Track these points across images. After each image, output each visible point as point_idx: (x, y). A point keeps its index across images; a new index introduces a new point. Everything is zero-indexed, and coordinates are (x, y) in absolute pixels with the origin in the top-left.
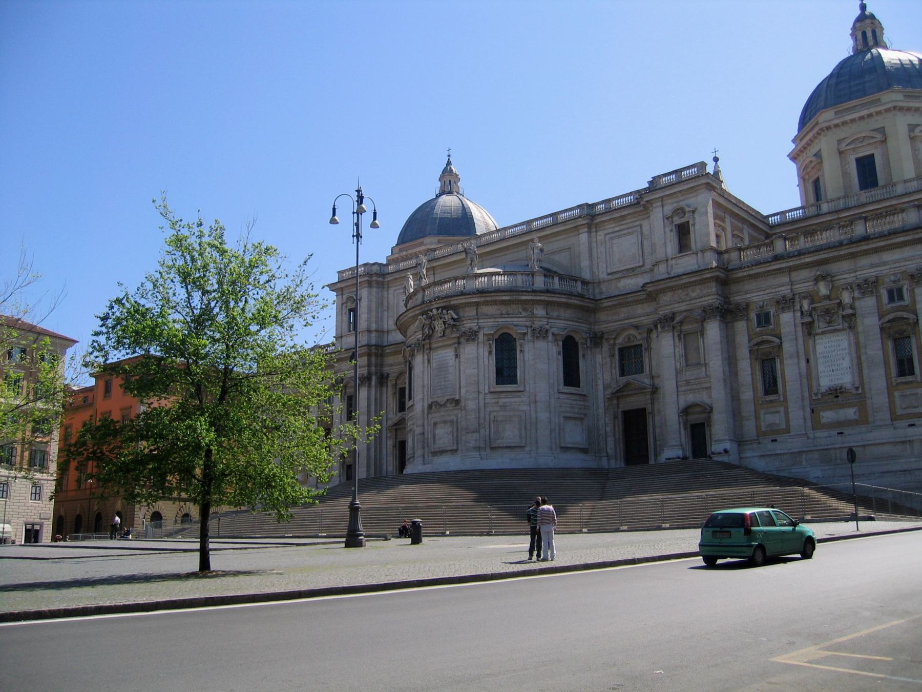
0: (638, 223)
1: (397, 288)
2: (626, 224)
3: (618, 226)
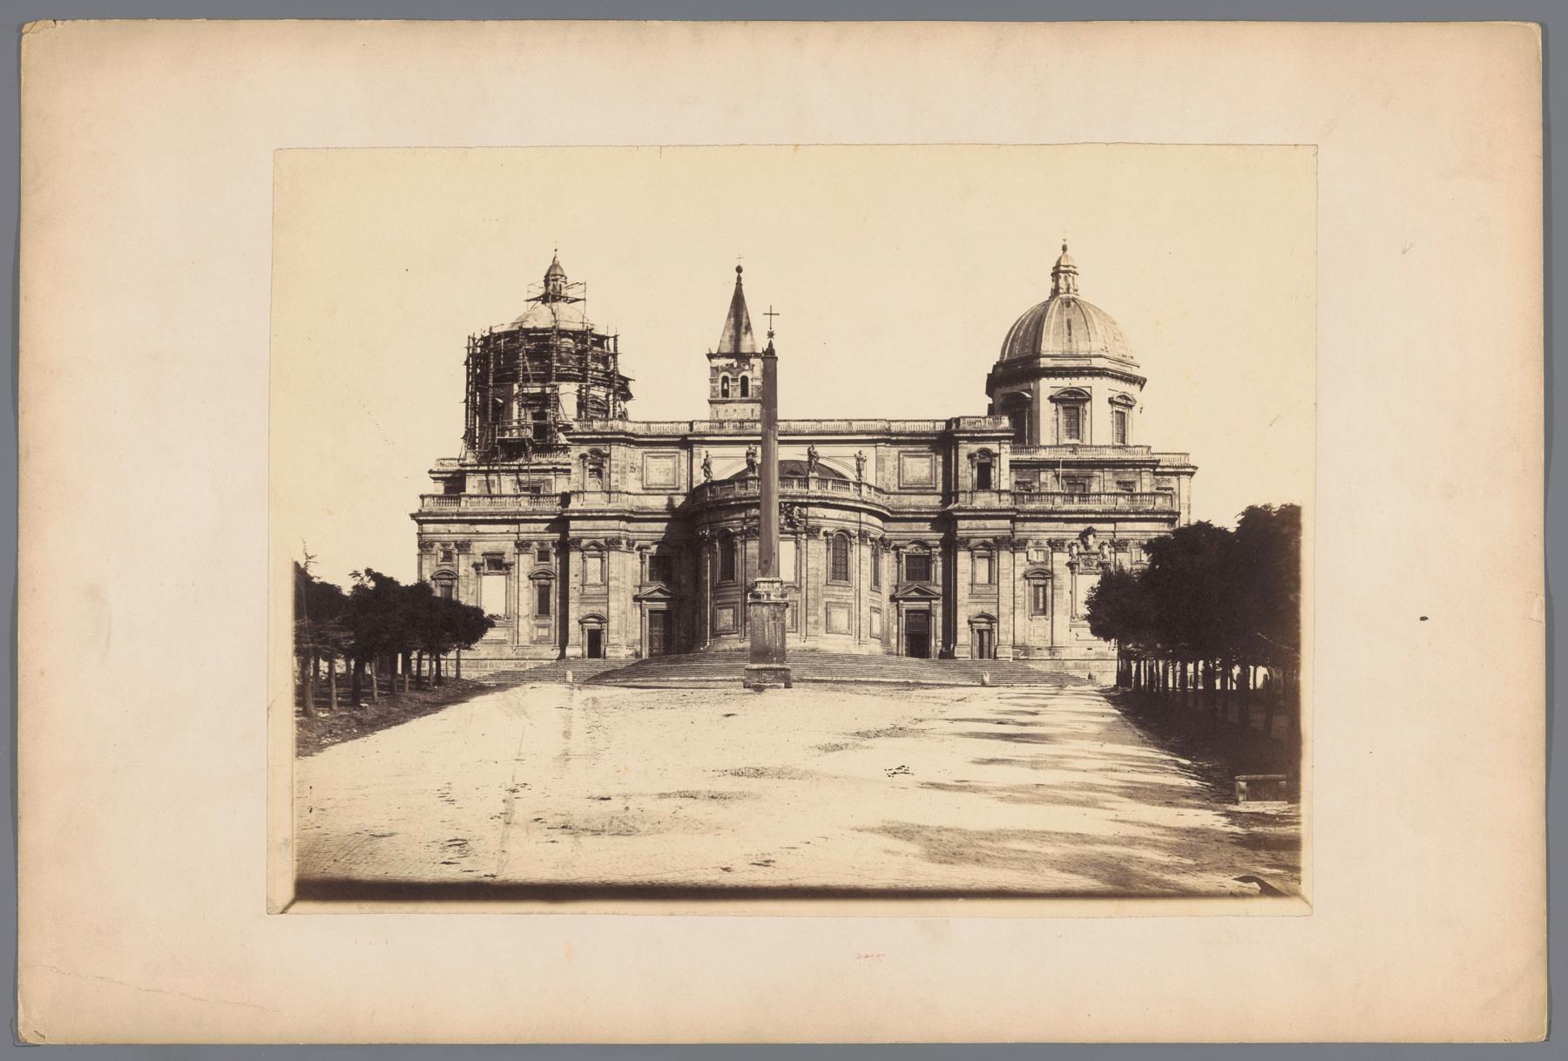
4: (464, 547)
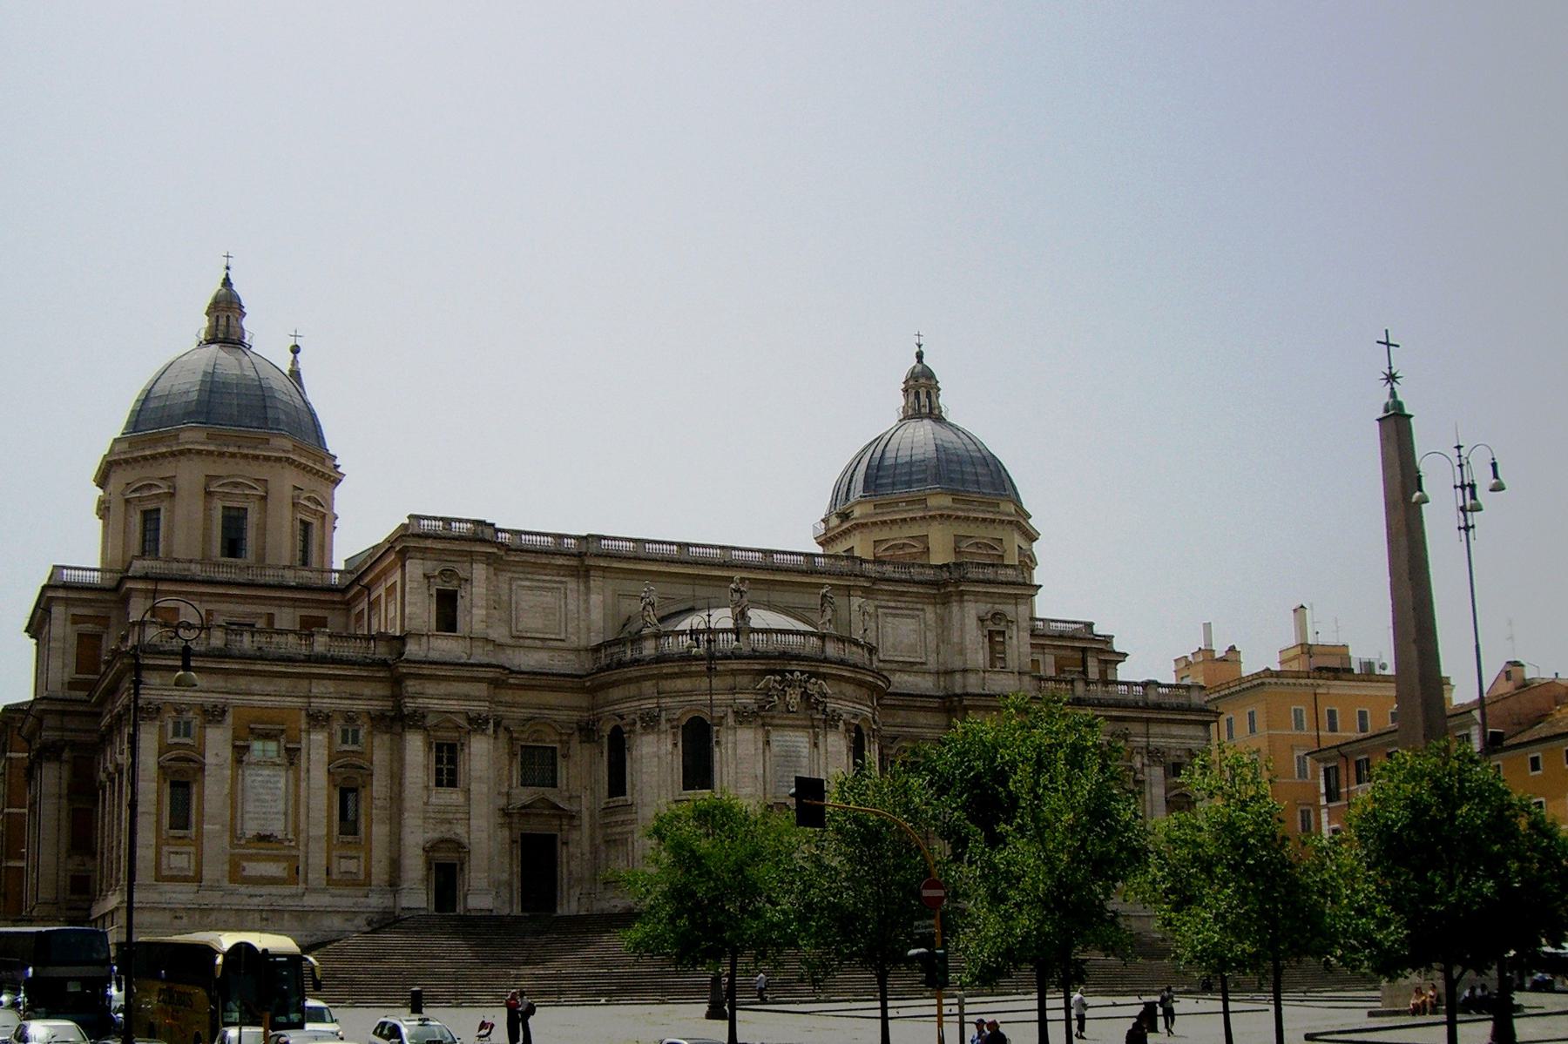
0: (919, 606)
1: (516, 576)
2: (905, 602)
3: (895, 601)
4: (214, 715)
